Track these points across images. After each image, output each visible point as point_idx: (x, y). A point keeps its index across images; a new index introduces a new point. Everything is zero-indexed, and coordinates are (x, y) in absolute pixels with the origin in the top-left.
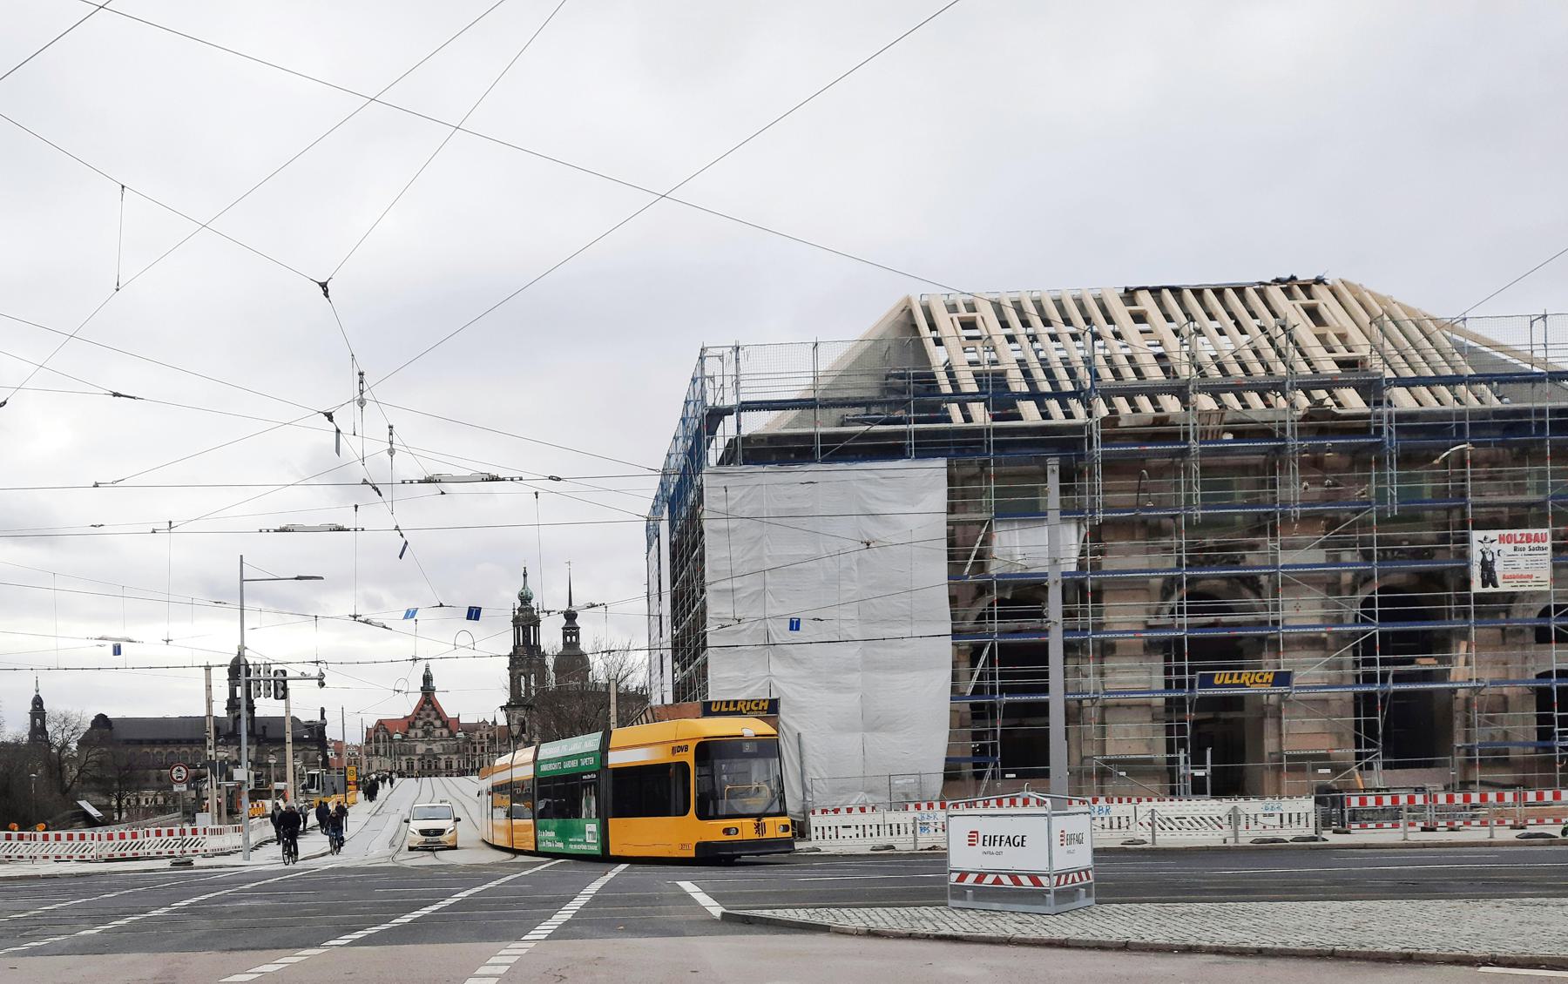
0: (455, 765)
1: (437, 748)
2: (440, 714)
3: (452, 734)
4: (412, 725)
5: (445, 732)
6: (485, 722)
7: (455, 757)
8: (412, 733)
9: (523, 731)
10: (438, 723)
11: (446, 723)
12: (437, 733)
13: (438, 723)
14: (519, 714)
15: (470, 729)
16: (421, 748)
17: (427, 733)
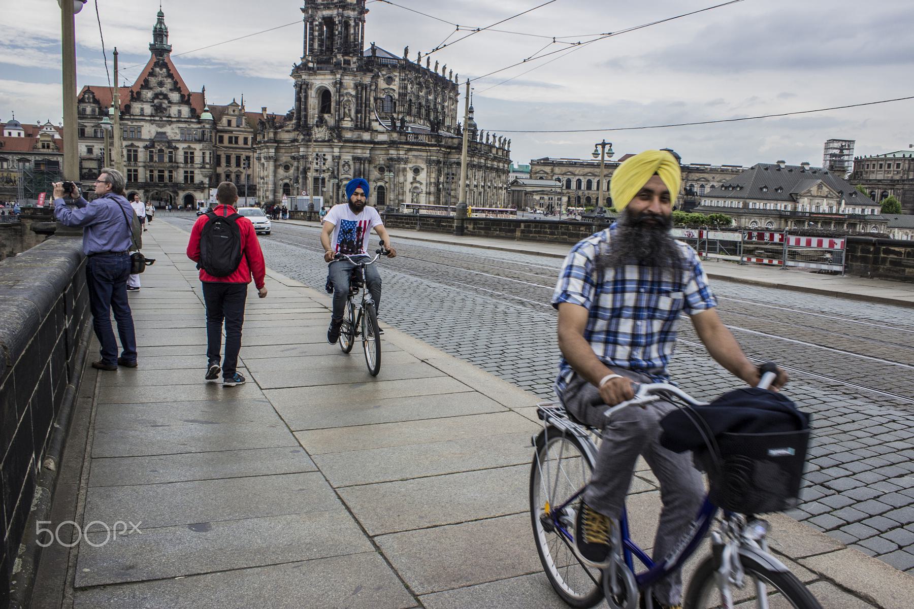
0: (198, 159)
1: (172, 131)
2: (177, 86)
3: (195, 114)
4: (136, 97)
5: (185, 110)
6: (234, 104)
7: (198, 147)
8: (136, 107)
9: (325, 107)
10: (175, 96)
11: (186, 99)
12: (174, 110)
13: (175, 96)
14: (324, 80)
15: (219, 113)
16: (149, 131)
17: (159, 109)
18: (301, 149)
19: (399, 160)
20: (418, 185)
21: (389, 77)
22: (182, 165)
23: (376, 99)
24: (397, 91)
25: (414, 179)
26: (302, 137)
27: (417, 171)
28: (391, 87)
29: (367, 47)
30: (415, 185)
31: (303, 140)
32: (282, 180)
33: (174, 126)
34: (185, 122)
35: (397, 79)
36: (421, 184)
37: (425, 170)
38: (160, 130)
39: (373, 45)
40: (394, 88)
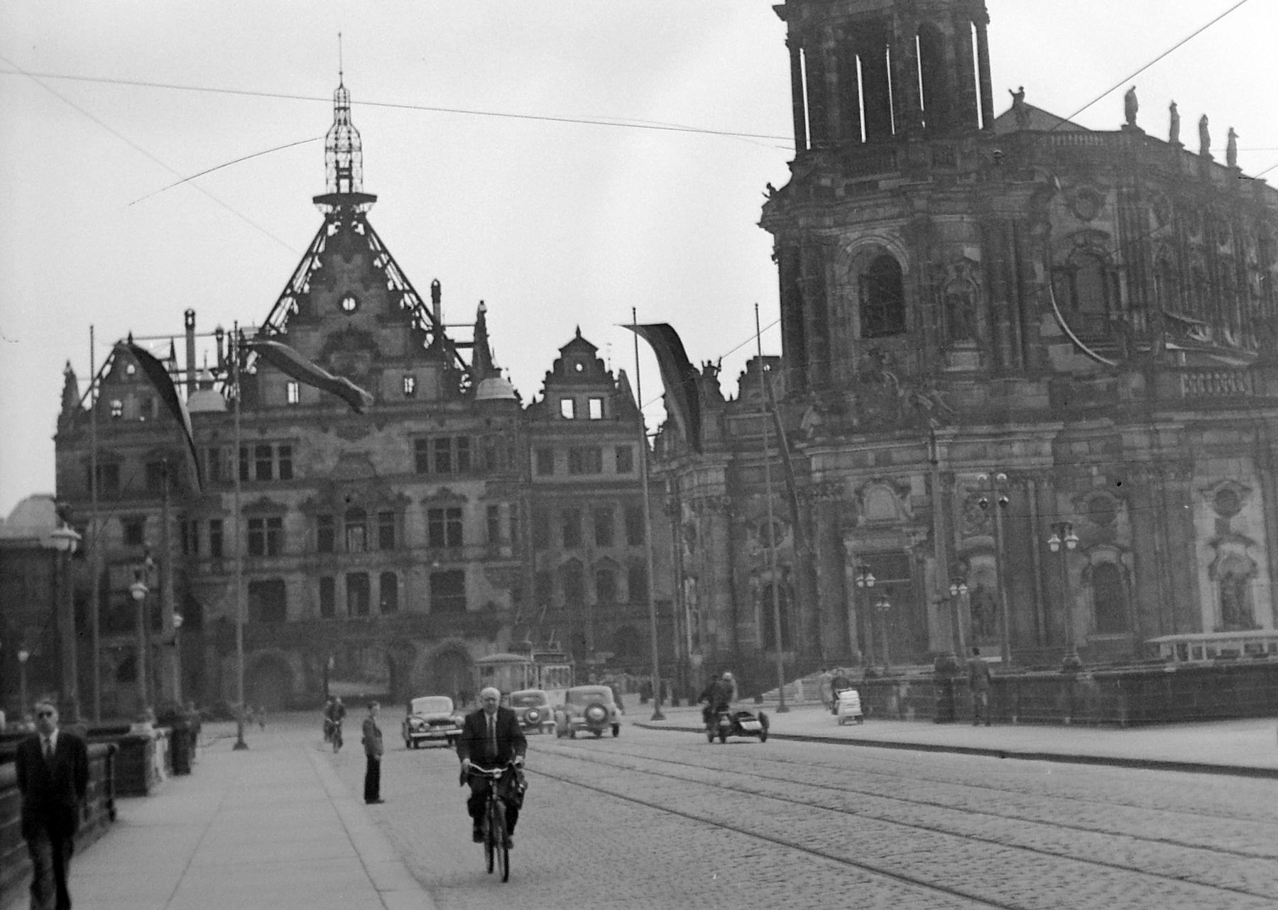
18: (815, 463)
19: (1159, 466)
20: (1238, 549)
21: (1084, 195)
22: (421, 555)
23: (1053, 270)
24: (1115, 236)
25: (1222, 528)
26: (815, 419)
27: (1228, 501)
28: (1096, 224)
29: (1002, 103)
30: (1227, 547)
31: (818, 430)
32: (754, 572)
33: (394, 430)
34: (431, 414)
35: (1111, 198)
36: (1249, 542)
37: (1257, 491)
38: (349, 446)
39: (1018, 96)
40: (1106, 226)
